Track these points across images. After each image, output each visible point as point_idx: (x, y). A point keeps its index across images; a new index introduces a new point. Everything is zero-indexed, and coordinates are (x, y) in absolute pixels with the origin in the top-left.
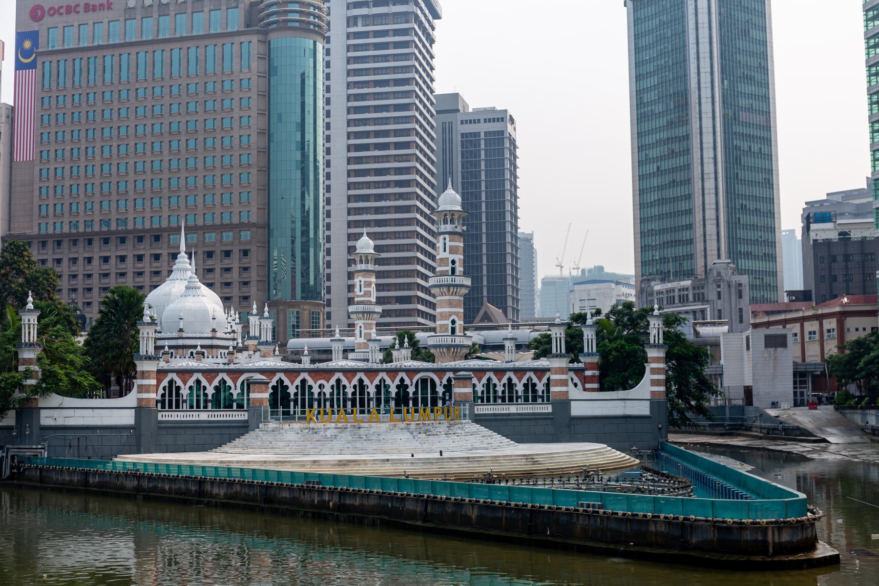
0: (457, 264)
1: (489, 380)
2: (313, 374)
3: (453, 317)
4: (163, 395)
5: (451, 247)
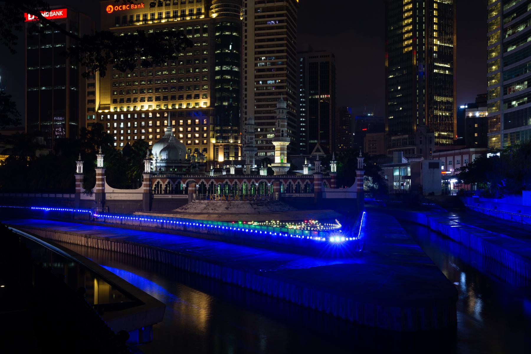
1: (290, 183)
4: (155, 188)
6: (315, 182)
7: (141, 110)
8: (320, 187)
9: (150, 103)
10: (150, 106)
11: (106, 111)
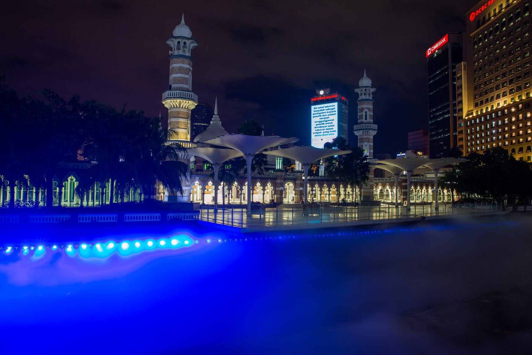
7: (497, 109)
9: (505, 99)
10: (505, 102)
11: (471, 116)
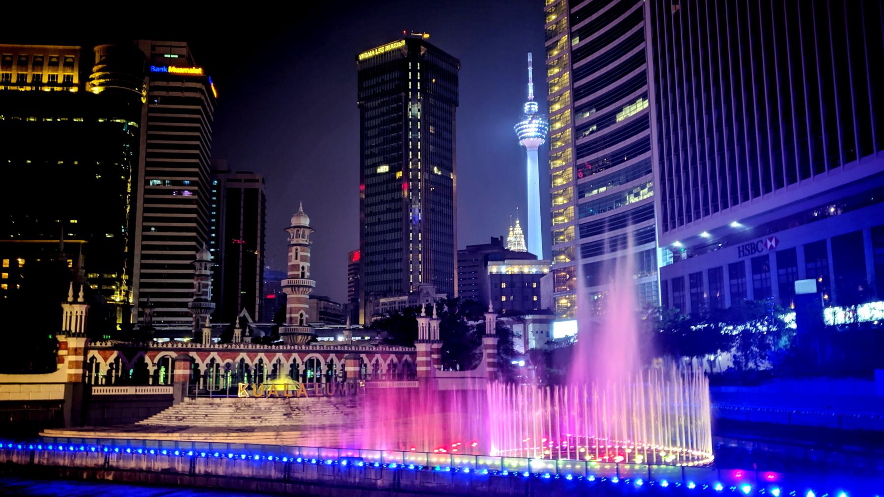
0: (306, 270)
2: (221, 353)
3: (302, 311)
5: (301, 256)
6: (419, 359)
8: (429, 368)
